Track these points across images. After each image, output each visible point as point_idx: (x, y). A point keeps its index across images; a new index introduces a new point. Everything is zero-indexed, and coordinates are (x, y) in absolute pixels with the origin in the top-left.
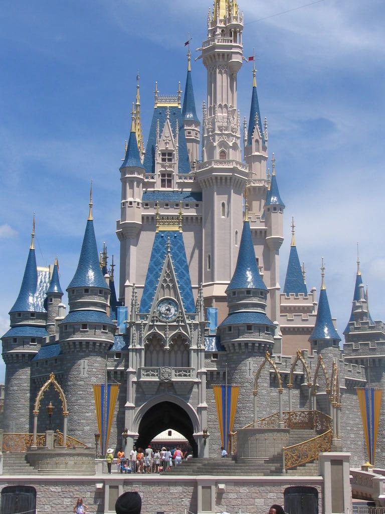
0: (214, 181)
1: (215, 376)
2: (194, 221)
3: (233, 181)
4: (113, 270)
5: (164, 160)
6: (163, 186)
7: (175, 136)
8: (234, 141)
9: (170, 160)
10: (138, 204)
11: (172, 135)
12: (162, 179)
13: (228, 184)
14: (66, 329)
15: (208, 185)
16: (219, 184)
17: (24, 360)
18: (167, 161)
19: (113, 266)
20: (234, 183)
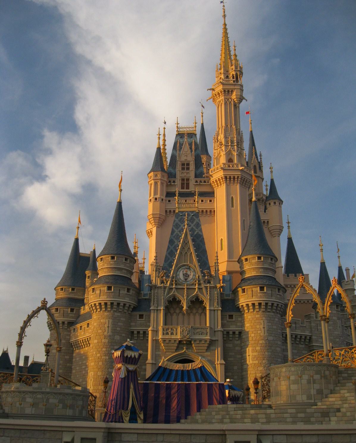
1: (231, 336)
2: (208, 213)
5: (183, 169)
7: (192, 151)
11: (189, 150)
12: (182, 183)
17: (64, 327)
18: (185, 169)
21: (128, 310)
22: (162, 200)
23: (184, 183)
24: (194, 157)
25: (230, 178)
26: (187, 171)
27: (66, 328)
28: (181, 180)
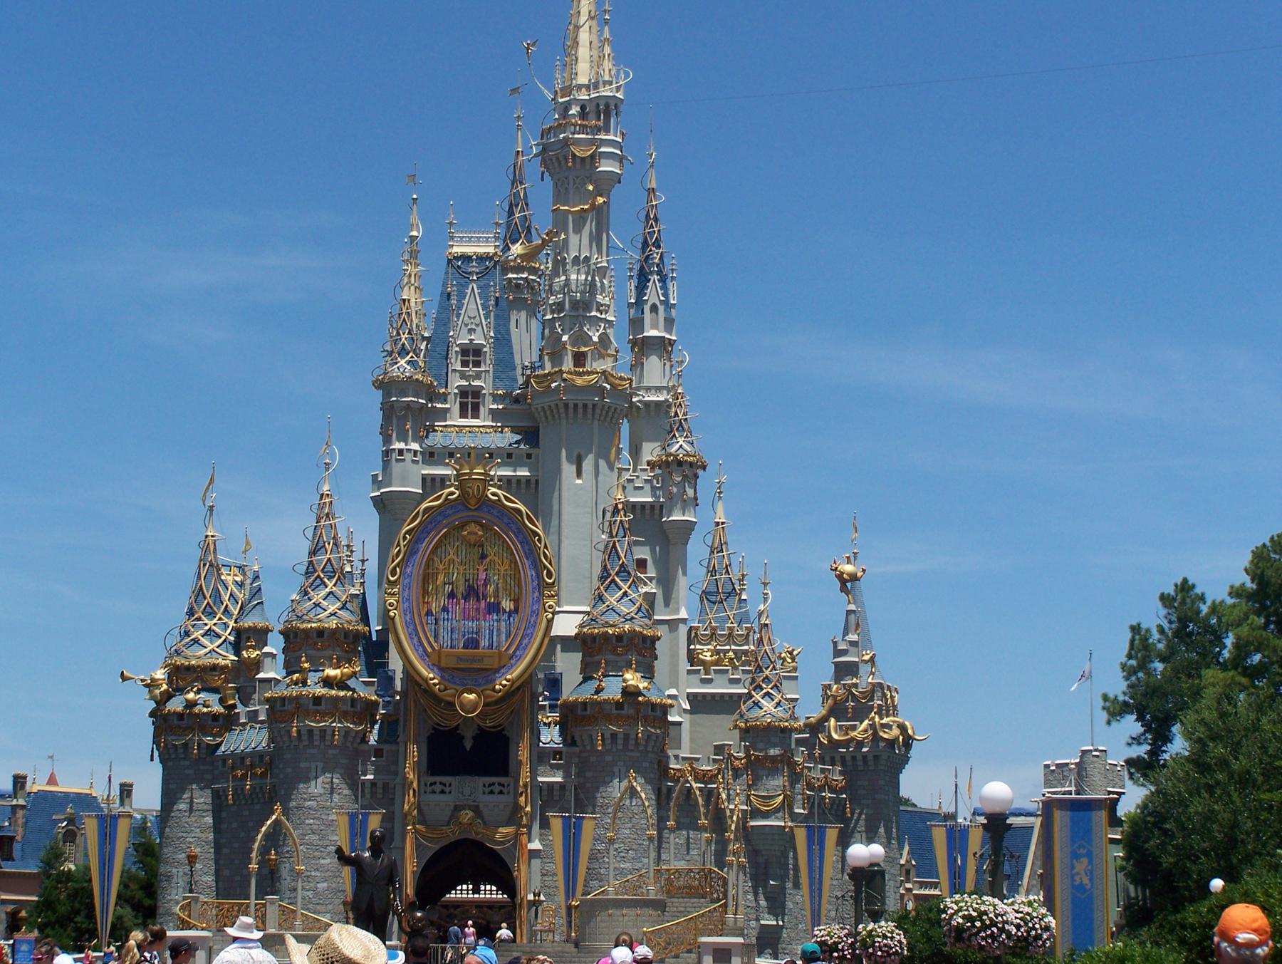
0: (562, 410)
3: (598, 411)
5: (464, 364)
6: (463, 415)
13: (590, 416)
14: (284, 705)
15: (550, 418)
16: (571, 415)
20: (600, 416)
21: (352, 743)
25: (576, 406)
27: (204, 756)
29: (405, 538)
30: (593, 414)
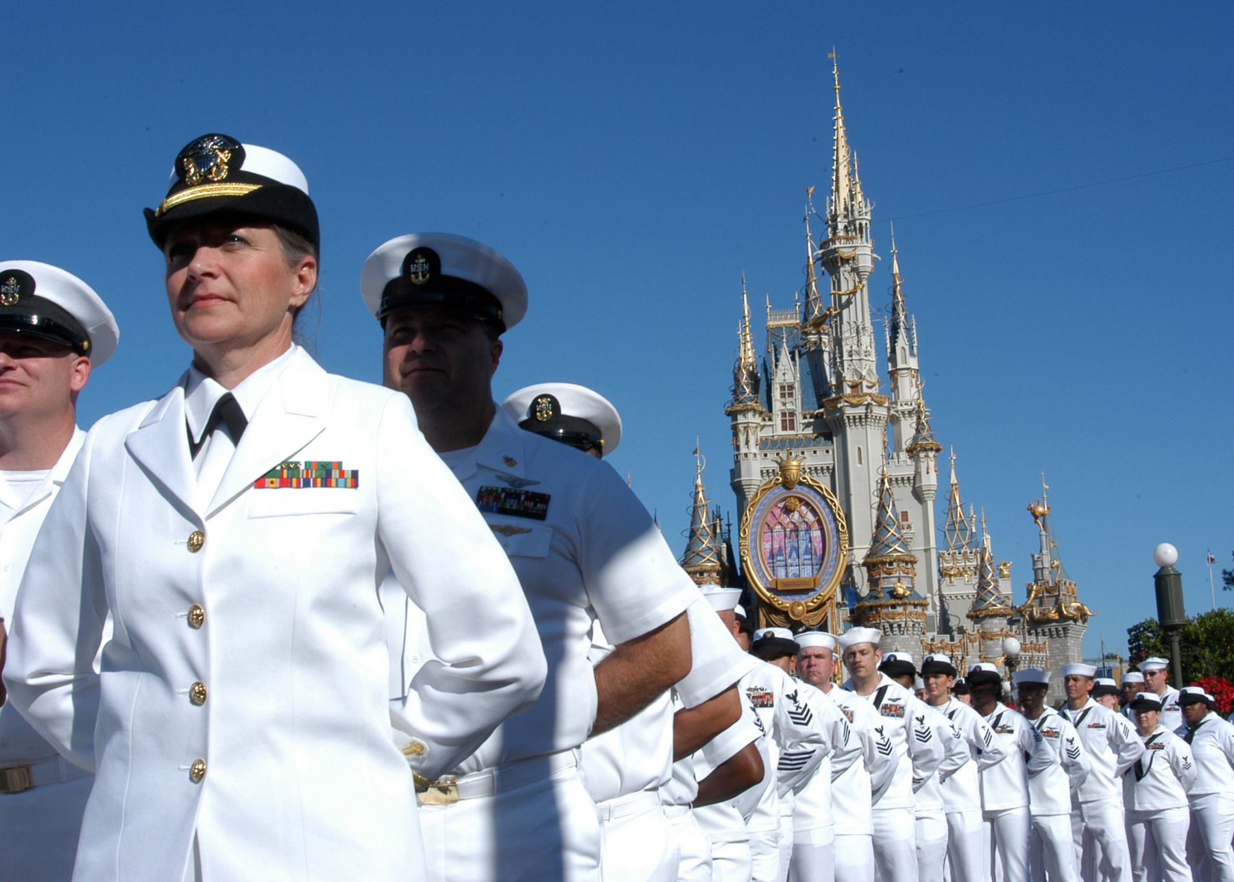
0: (847, 421)
4: (729, 531)
5: (783, 395)
8: (867, 367)
9: (791, 395)
10: (755, 454)
12: (782, 420)
15: (839, 426)
18: (787, 396)
19: (729, 525)
22: (755, 454)
23: (786, 420)
24: (798, 375)
26: (791, 399)
28: (780, 416)
29: (750, 510)
30: (866, 421)
